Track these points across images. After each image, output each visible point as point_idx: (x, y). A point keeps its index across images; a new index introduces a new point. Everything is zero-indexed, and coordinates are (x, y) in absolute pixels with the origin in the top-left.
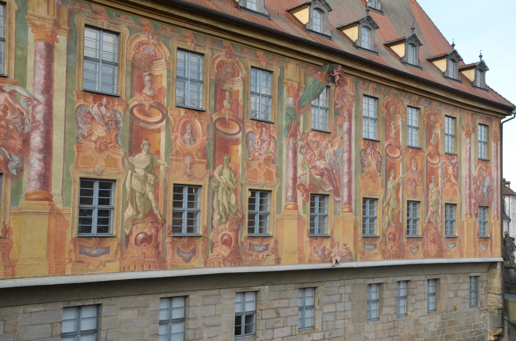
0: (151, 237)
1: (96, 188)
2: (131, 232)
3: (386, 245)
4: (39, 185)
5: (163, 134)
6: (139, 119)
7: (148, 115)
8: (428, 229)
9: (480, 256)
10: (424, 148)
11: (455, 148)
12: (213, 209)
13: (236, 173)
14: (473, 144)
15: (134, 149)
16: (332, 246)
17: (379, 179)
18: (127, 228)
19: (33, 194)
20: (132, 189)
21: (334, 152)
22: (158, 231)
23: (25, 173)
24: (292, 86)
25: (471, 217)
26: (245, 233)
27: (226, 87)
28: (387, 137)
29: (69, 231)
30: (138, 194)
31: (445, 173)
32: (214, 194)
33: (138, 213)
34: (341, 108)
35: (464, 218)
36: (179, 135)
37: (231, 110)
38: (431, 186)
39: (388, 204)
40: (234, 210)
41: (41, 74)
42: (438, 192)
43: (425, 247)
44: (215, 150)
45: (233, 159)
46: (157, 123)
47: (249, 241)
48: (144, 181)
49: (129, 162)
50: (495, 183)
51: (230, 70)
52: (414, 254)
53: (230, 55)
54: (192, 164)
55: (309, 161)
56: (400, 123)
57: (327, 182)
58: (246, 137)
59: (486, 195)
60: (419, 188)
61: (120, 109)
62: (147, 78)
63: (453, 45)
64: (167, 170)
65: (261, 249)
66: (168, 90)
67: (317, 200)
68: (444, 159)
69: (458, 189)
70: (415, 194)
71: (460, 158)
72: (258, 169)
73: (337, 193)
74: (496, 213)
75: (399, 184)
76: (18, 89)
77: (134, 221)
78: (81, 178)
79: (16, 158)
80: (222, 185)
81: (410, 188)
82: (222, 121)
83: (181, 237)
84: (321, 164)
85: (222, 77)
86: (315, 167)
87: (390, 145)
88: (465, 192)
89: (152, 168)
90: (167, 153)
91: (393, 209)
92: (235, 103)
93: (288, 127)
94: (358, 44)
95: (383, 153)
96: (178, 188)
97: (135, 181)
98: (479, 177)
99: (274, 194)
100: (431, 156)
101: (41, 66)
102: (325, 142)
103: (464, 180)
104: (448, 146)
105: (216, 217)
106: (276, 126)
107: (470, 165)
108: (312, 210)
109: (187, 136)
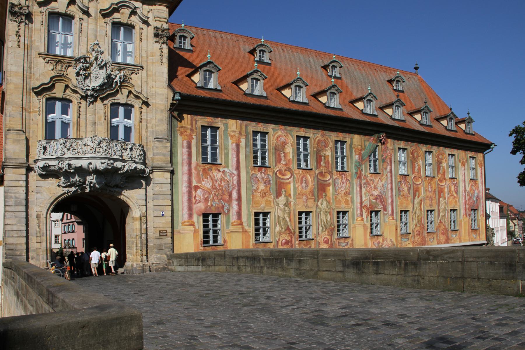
0: (288, 241)
1: (261, 217)
2: (279, 239)
3: (414, 238)
4: (237, 217)
5: (292, 185)
6: (280, 178)
7: (284, 175)
8: (440, 226)
9: (472, 241)
10: (436, 177)
11: (455, 174)
12: (319, 224)
13: (329, 203)
14: (466, 170)
15: (278, 194)
16: (383, 241)
17: (410, 199)
18: (277, 237)
19: (235, 222)
20: (278, 216)
21: (383, 185)
22: (292, 238)
23: (231, 212)
24: (357, 148)
25: (467, 217)
26: (336, 237)
27: (322, 154)
28: (413, 172)
29: (251, 240)
30: (281, 219)
31: (450, 190)
32: (318, 215)
33: (282, 228)
34: (386, 158)
35: (462, 218)
36: (300, 184)
37: (325, 167)
38: (441, 199)
39: (415, 213)
40: (329, 224)
41: (235, 159)
42: (446, 203)
44: (318, 191)
45: (328, 195)
46: (289, 179)
47: (338, 240)
48: (284, 211)
49: (276, 202)
50: (481, 194)
51: (323, 144)
52: (432, 242)
53: (323, 135)
54: (307, 200)
55: (369, 192)
56: (421, 162)
57: (379, 203)
58: (334, 181)
60: (434, 201)
61: (271, 173)
62: (283, 155)
63: (451, 109)
64: (295, 204)
65: (344, 245)
66: (293, 160)
67: (373, 214)
68: (448, 182)
70: (431, 205)
71: (459, 181)
72: (341, 199)
73: (385, 209)
74: (482, 213)
75: (421, 201)
76: (226, 169)
77: (280, 233)
78: (255, 213)
79: (227, 205)
80: (323, 210)
81: (428, 202)
82: (321, 174)
83: (303, 240)
84: (375, 193)
85: (320, 149)
86: (372, 195)
87: (415, 177)
88: (462, 201)
89: (287, 204)
90: (294, 195)
91: (418, 216)
93: (356, 173)
94: (393, 117)
95: (411, 182)
96: (300, 213)
97: (280, 212)
98: (471, 191)
99: (350, 212)
100: (440, 181)
101: (235, 156)
102: (377, 179)
103: (461, 193)
104: (450, 173)
105: (321, 228)
106: (349, 173)
107: (465, 184)
108: (371, 221)
109: (304, 185)
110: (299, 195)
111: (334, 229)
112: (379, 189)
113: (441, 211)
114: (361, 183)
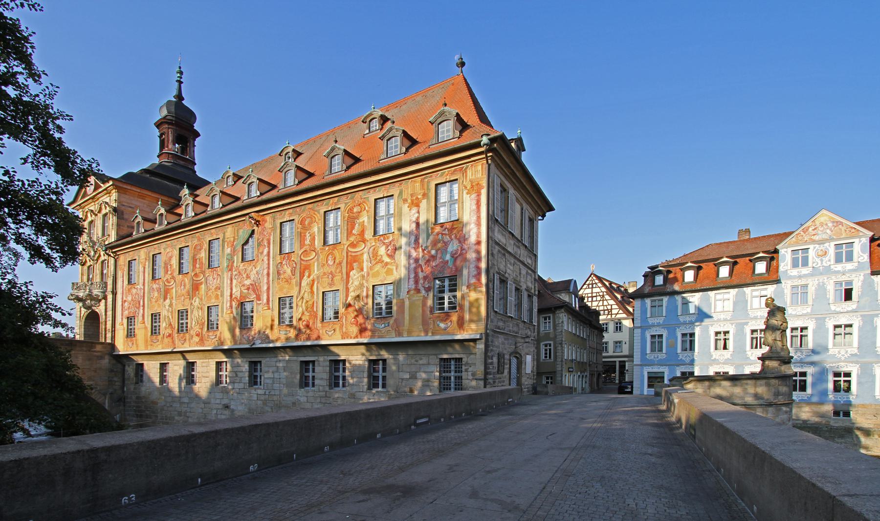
13: (201, 299)
15: (165, 299)
39: (302, 298)
43: (344, 330)
48: (168, 311)
57: (252, 293)
59: (450, 264)
60: (337, 278)
69: (394, 268)
75: (313, 281)
81: (326, 280)
84: (248, 282)
89: (171, 305)
92: (201, 263)
95: (297, 260)
100: (353, 245)
110: (178, 297)
111: (204, 324)
112: (252, 277)
113: (351, 289)
114: (232, 275)
